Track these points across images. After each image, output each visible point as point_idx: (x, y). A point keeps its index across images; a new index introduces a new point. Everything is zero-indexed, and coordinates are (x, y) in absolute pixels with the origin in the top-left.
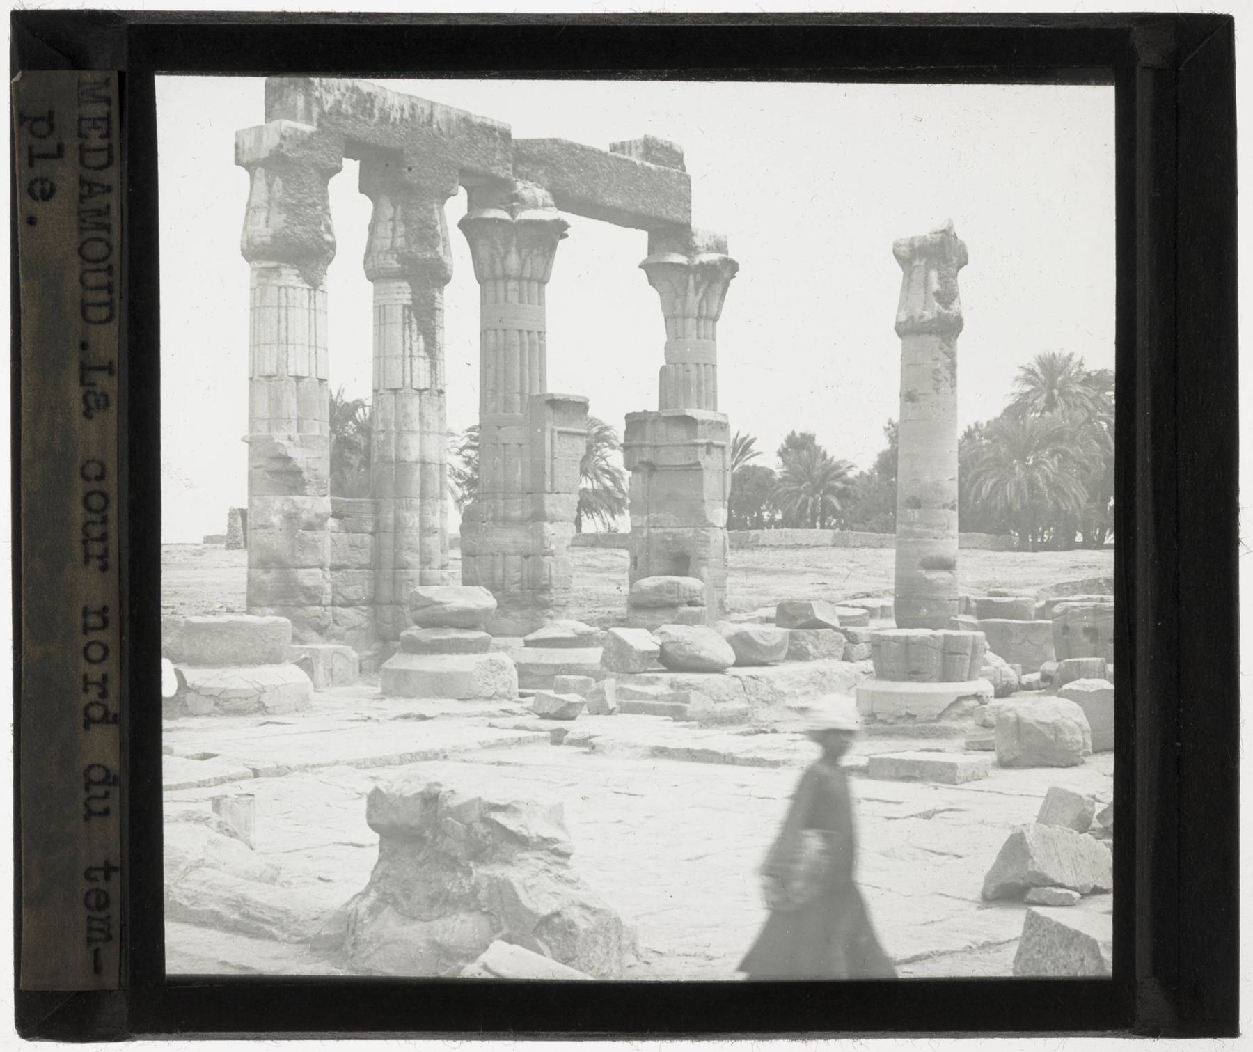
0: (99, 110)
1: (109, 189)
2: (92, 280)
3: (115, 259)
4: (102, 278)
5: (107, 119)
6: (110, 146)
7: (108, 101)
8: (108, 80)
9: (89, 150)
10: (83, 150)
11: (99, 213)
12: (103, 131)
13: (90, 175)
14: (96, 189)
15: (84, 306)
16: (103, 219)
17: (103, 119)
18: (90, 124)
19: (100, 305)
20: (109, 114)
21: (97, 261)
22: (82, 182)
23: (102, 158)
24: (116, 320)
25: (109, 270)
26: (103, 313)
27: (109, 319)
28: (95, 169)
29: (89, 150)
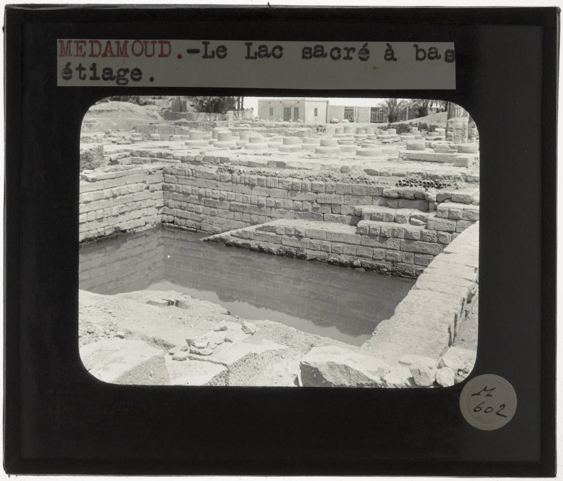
0: (73, 46)
1: (109, 43)
2: (150, 52)
3: (142, 41)
4: (150, 46)
5: (77, 42)
6: (90, 42)
7: (69, 42)
8: (60, 42)
9: (92, 52)
10: (92, 55)
11: (118, 48)
12: (83, 44)
13: (103, 52)
14: (109, 49)
15: (162, 55)
16: (122, 45)
17: (78, 45)
18: (79, 51)
19: (162, 47)
20: (75, 42)
21: (143, 48)
22: (105, 55)
23: (96, 46)
24: (169, 40)
25: (146, 43)
26: (166, 46)
27: (169, 43)
28: (100, 49)
29: (92, 52)
